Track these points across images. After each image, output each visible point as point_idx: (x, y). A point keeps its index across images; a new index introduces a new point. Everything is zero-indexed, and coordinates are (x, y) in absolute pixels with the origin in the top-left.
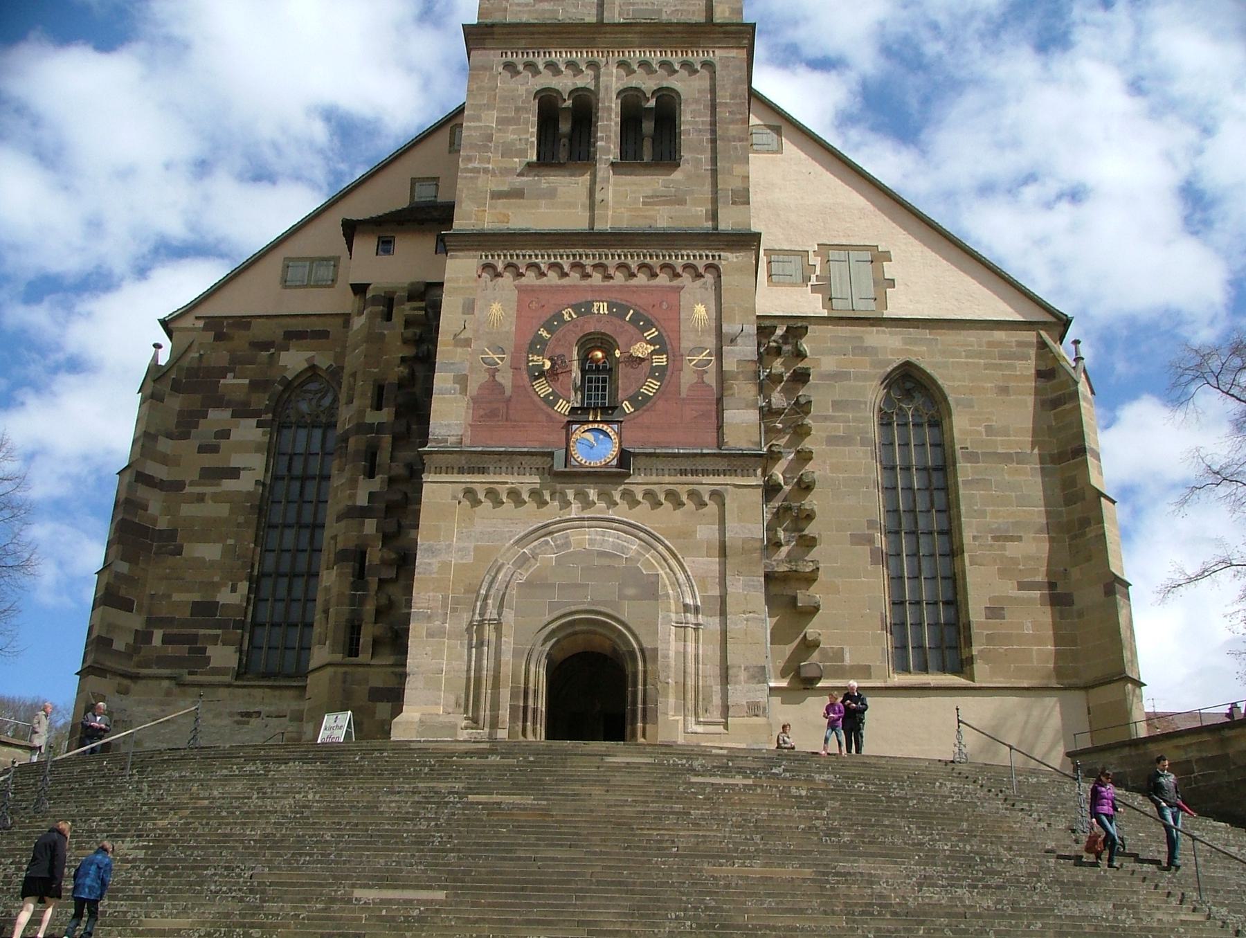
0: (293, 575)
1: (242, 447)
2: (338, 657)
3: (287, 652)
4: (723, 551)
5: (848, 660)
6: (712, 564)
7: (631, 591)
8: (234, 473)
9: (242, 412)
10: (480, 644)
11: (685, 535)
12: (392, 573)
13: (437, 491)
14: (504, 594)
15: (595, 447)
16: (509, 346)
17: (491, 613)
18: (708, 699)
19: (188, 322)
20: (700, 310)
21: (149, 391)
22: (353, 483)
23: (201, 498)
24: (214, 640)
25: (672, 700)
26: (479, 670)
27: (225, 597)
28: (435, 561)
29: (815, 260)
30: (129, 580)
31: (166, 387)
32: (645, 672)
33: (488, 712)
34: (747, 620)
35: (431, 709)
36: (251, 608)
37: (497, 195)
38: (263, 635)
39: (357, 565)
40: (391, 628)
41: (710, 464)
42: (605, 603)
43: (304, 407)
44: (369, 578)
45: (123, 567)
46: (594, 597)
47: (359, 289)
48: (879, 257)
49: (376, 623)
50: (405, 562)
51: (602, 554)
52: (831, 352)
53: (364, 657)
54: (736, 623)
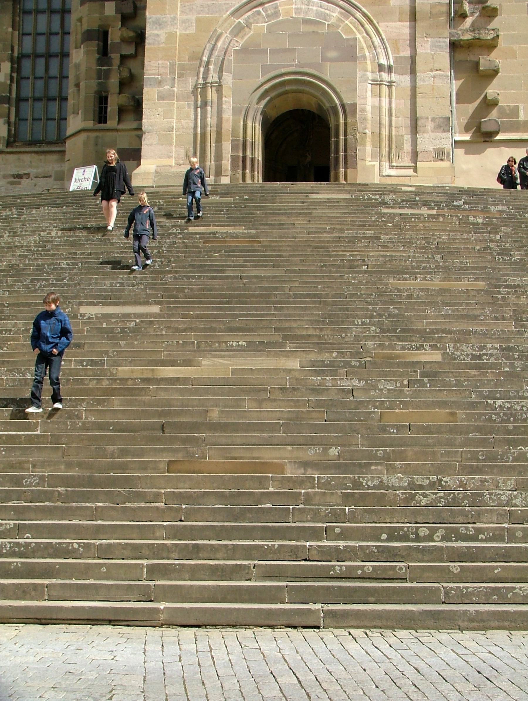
0: (48, 56)
2: (90, 124)
3: (49, 122)
4: (413, 16)
5: (522, 116)
6: (405, 28)
7: (332, 54)
10: (205, 104)
14: (223, 60)
17: (213, 77)
18: (399, 147)
25: (369, 148)
26: (204, 126)
28: (162, 33)
32: (346, 124)
33: (213, 163)
34: (434, 77)
35: (165, 162)
36: (14, 86)
38: (27, 108)
39: (101, 44)
40: (133, 97)
42: (310, 65)
44: (113, 55)
49: (119, 94)
50: (139, 39)
51: (307, 22)
53: (112, 123)
54: (424, 79)
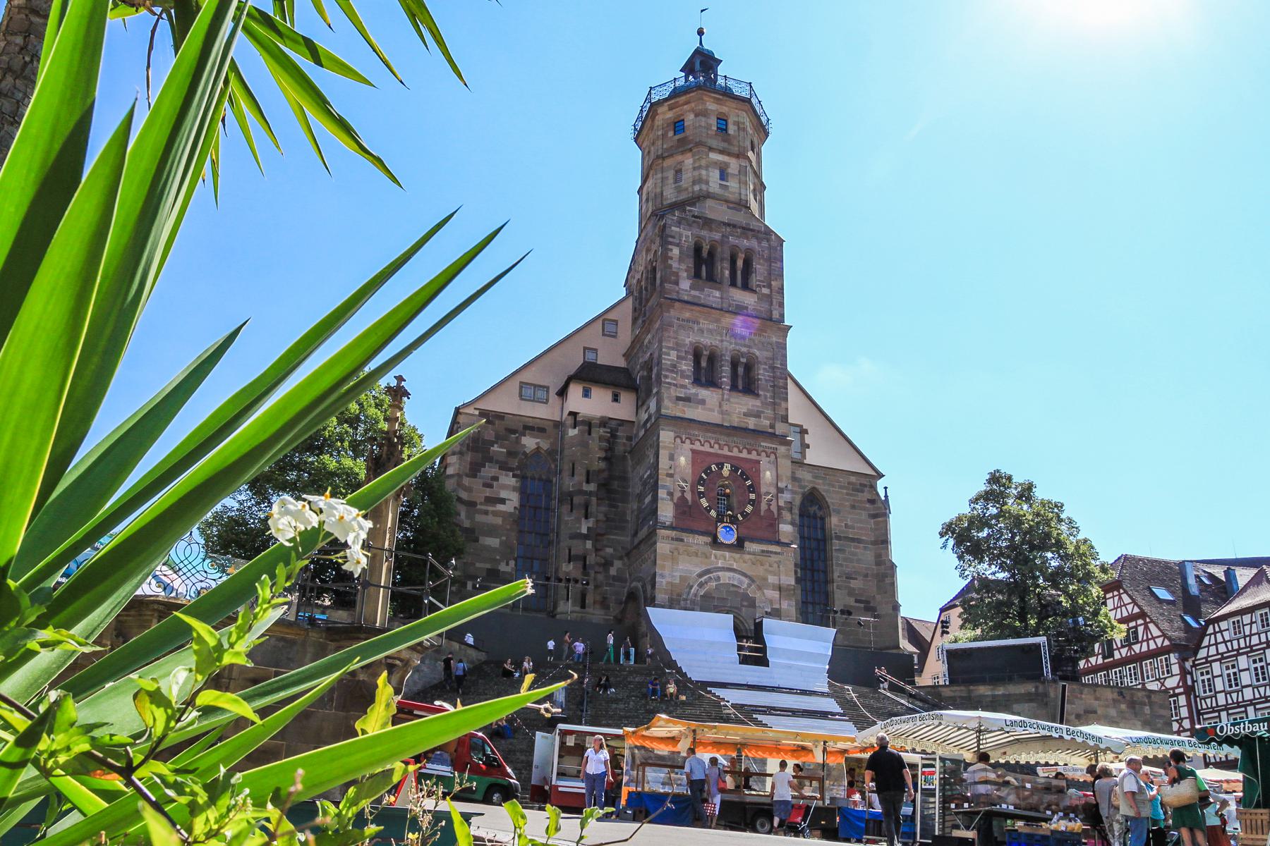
1: (505, 487)
2: (578, 609)
8: (503, 501)
9: (504, 467)
11: (766, 579)
12: (601, 569)
15: (727, 536)
16: (689, 479)
20: (768, 473)
23: (486, 513)
37: (679, 399)
48: (803, 432)
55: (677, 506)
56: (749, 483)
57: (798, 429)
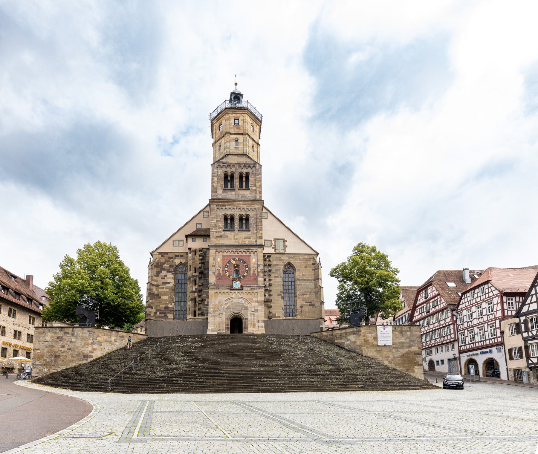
1: (169, 278)
2: (192, 317)
8: (169, 283)
9: (168, 271)
13: (211, 292)
15: (237, 284)
16: (221, 266)
19: (156, 253)
21: (150, 267)
22: (192, 286)
23: (163, 288)
24: (169, 313)
27: (170, 306)
29: (273, 242)
30: (152, 303)
31: (153, 266)
38: (177, 312)
41: (255, 288)
43: (180, 270)
45: (151, 301)
46: (238, 310)
47: (190, 249)
48: (285, 241)
52: (275, 260)
55: (216, 276)
56: (246, 264)
57: (283, 241)
